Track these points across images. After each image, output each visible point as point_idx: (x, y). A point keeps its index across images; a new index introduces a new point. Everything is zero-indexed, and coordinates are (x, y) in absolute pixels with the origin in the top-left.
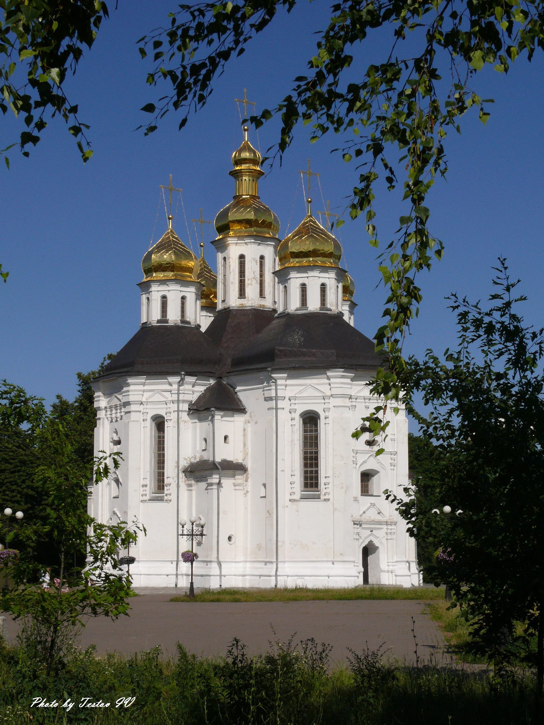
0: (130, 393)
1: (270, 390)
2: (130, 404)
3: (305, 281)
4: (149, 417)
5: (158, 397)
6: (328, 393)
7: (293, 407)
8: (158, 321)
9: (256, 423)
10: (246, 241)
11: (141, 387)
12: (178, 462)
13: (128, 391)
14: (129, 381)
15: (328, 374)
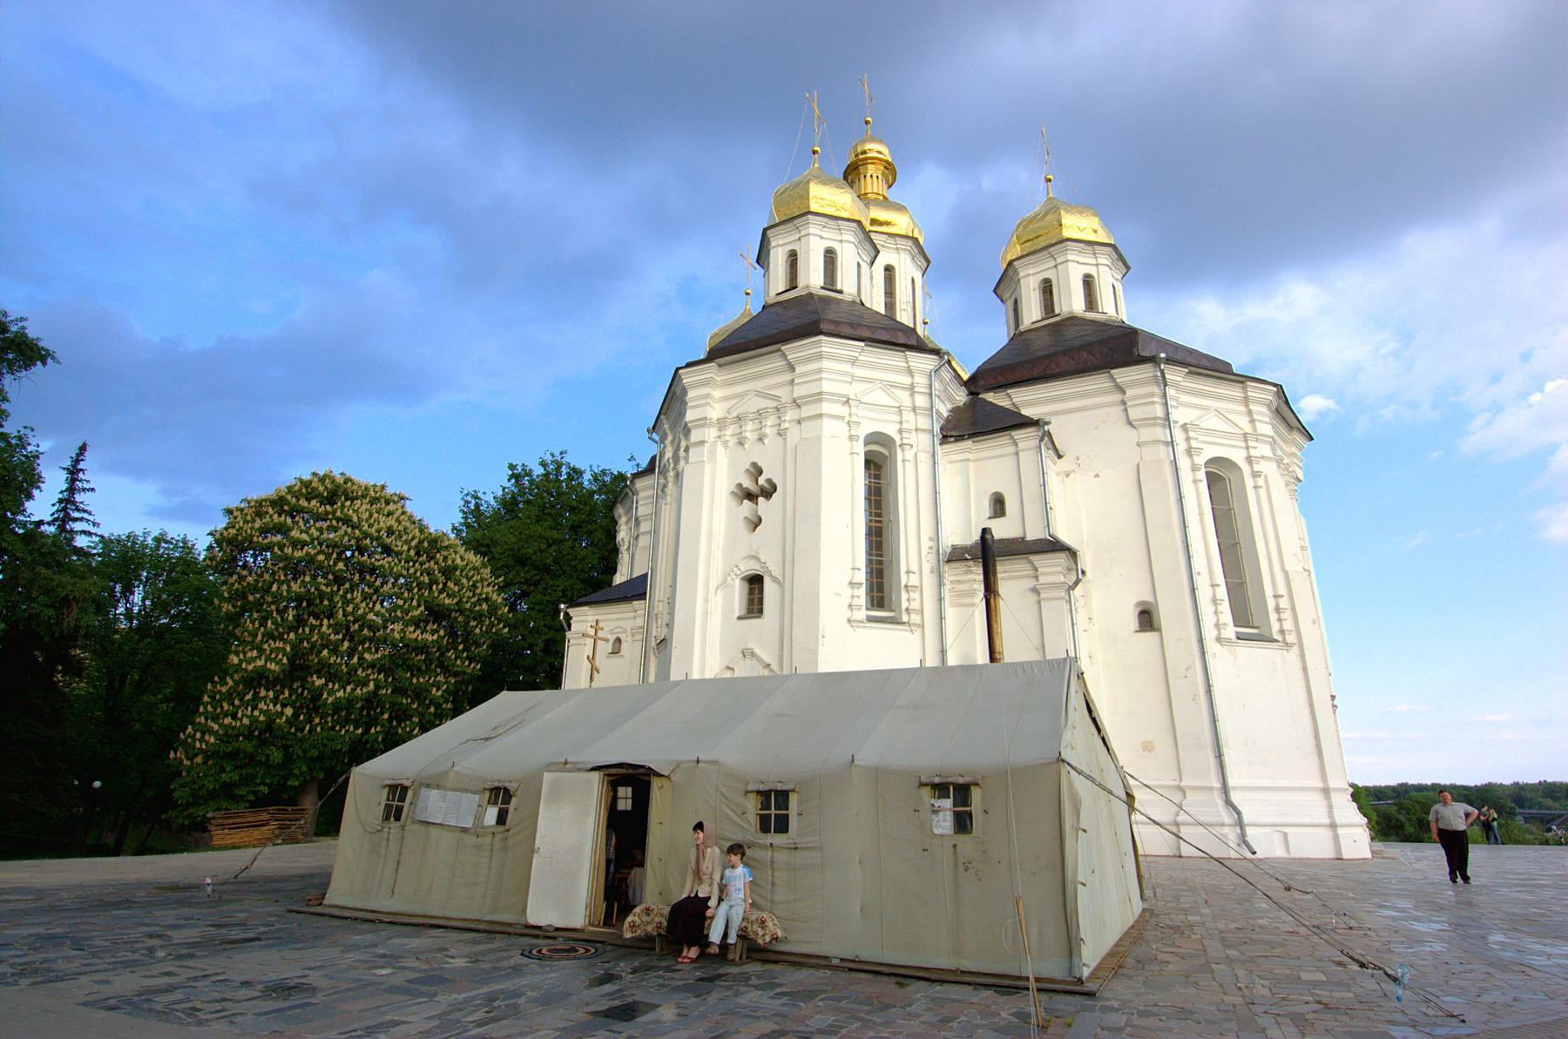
0: (824, 375)
1: (1153, 403)
2: (821, 400)
3: (1092, 271)
4: (863, 432)
5: (879, 397)
6: (1248, 429)
7: (1194, 444)
8: (823, 288)
9: (1097, 476)
10: (899, 246)
11: (847, 368)
12: (937, 537)
13: (820, 371)
14: (823, 349)
15: (1249, 394)
